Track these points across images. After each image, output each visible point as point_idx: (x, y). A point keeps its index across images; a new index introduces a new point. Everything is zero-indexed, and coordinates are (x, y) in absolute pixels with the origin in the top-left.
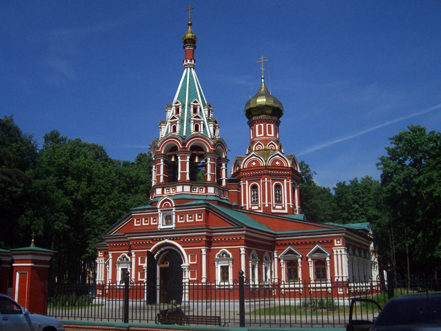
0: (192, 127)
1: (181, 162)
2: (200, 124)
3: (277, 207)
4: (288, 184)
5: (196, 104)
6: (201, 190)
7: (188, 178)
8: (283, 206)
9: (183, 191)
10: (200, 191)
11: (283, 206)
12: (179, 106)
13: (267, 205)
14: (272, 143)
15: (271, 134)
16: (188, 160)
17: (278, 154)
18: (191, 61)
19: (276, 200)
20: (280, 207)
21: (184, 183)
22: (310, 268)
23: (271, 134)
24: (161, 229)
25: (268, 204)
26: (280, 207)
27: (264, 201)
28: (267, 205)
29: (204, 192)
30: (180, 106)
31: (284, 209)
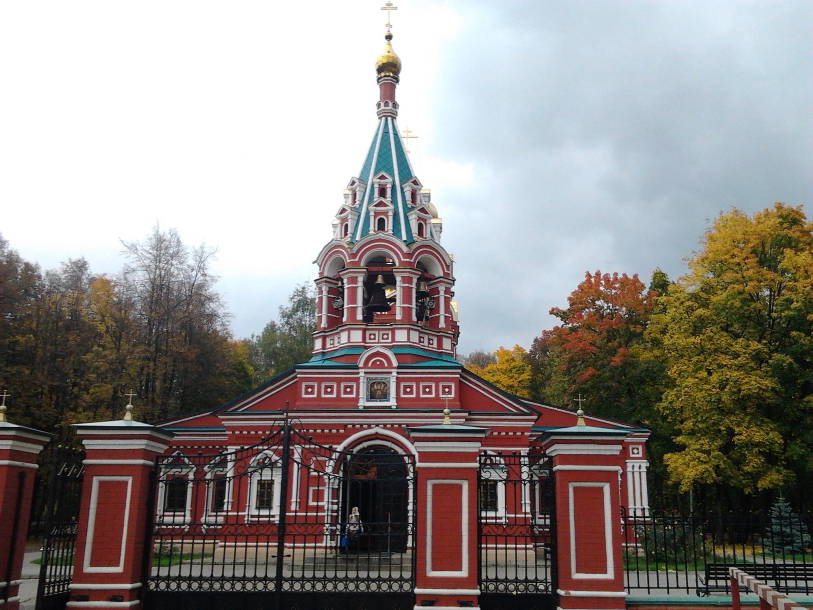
0: (373, 226)
1: (348, 288)
2: (387, 218)
5: (383, 181)
7: (360, 317)
9: (349, 342)
10: (383, 339)
12: (356, 188)
18: (386, 104)
21: (353, 323)
22: (160, 489)
24: (365, 407)
29: (390, 340)
30: (358, 189)
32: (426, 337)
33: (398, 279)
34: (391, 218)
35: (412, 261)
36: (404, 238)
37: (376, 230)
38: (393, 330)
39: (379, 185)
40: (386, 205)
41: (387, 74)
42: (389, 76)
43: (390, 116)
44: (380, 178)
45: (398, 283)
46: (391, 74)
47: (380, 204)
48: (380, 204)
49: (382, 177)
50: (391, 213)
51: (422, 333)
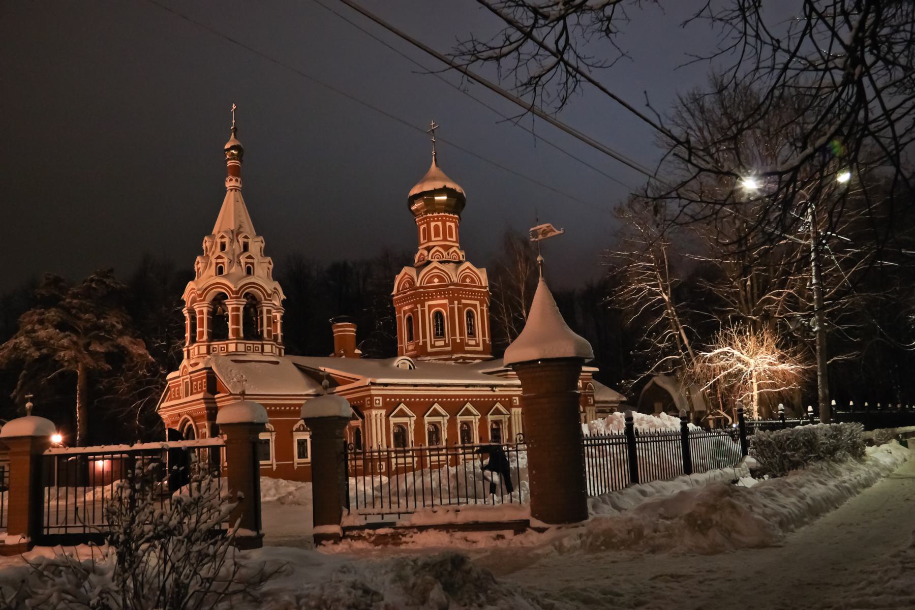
3: (437, 344)
4: (452, 310)
6: (223, 349)
7: (205, 337)
8: (447, 342)
11: (447, 342)
13: (421, 344)
14: (437, 251)
15: (439, 236)
17: (436, 268)
19: (437, 334)
20: (442, 343)
23: (439, 236)
25: (460, 339)
26: (442, 343)
27: (454, 334)
28: (421, 344)
31: (446, 345)
32: (251, 345)
35: (239, 296)
38: (227, 344)
47: (219, 257)
48: (219, 257)
51: (245, 344)
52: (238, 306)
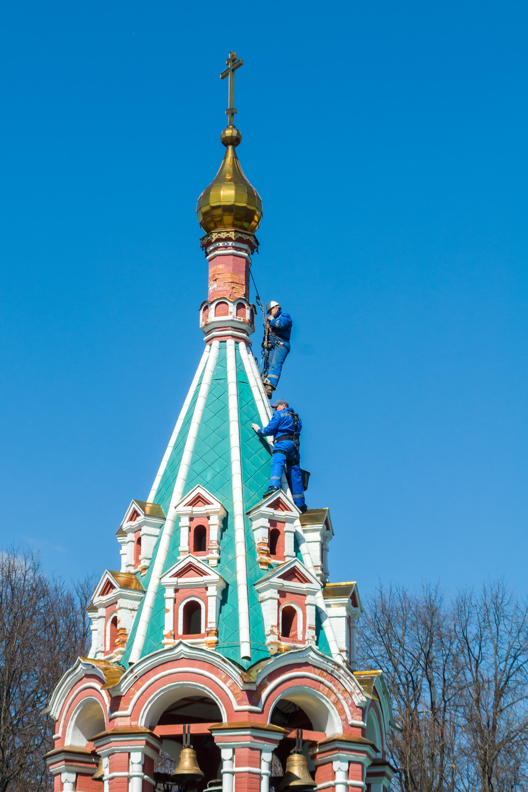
16: (136, 769)
33: (226, 754)
34: (213, 603)
36: (245, 650)
37: (180, 631)
39: (191, 519)
40: (202, 573)
41: (223, 235)
42: (228, 239)
43: (233, 337)
44: (193, 503)
45: (227, 766)
46: (232, 235)
47: (189, 568)
49: (198, 500)
50: (213, 591)
52: (260, 744)
